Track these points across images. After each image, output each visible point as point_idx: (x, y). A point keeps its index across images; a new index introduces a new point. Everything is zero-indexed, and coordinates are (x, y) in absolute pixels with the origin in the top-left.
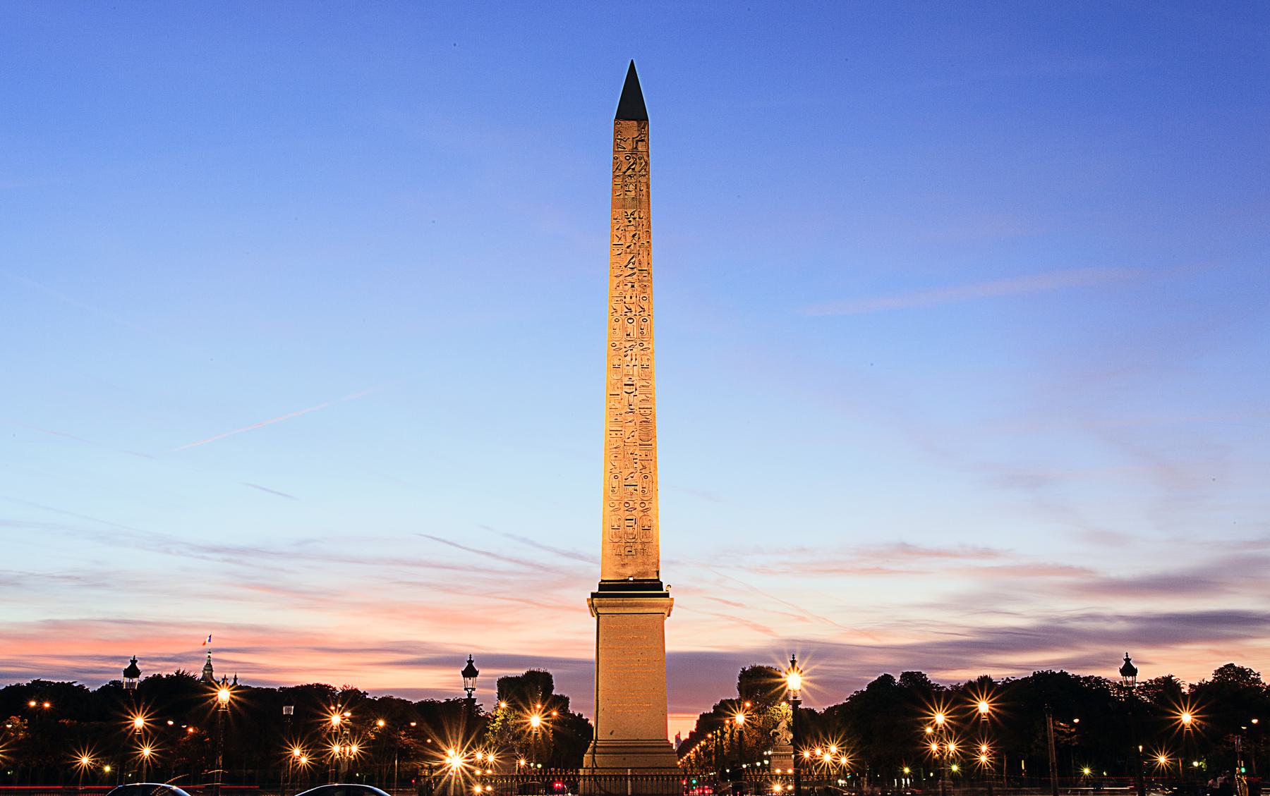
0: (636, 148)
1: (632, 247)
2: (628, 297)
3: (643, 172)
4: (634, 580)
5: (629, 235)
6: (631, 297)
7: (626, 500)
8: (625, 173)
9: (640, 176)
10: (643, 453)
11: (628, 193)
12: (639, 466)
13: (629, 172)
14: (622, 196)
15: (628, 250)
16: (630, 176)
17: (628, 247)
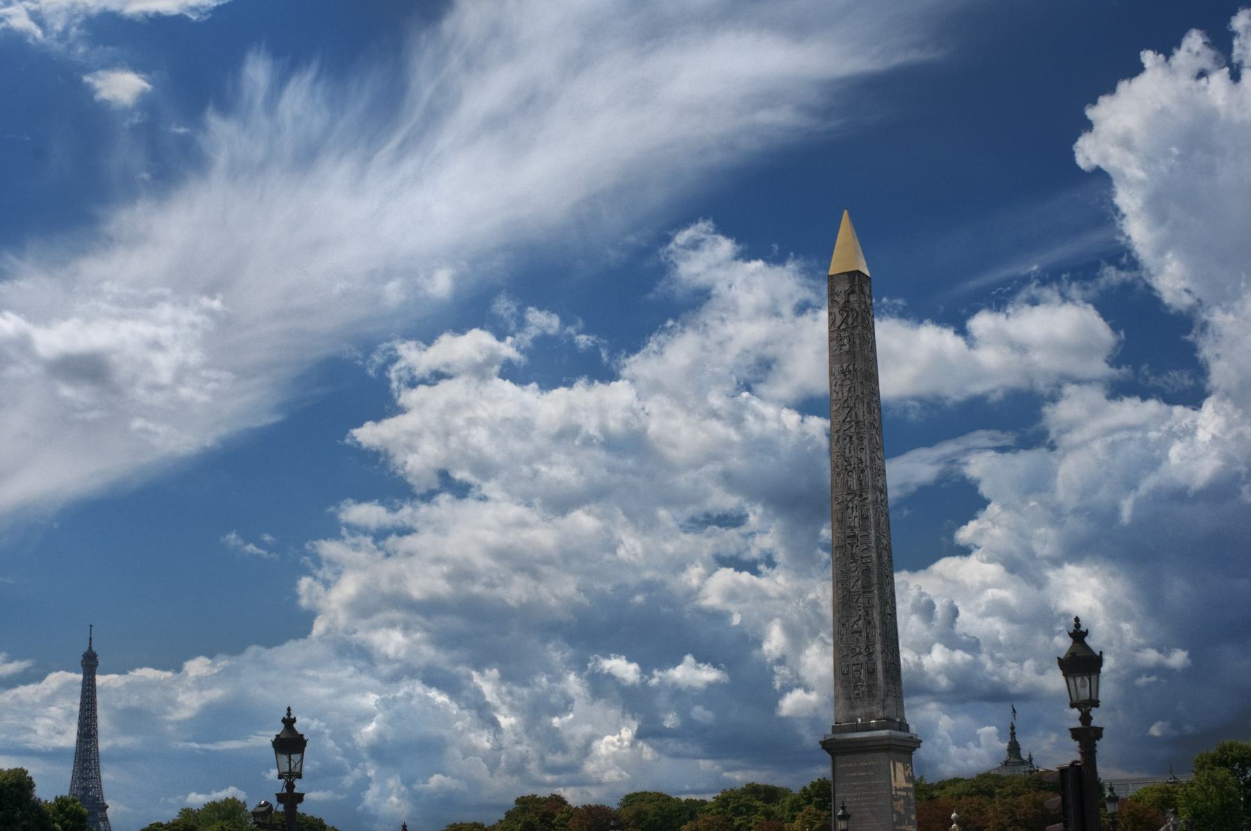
0: (848, 301)
2: (847, 451)
3: (855, 324)
5: (845, 389)
6: (850, 452)
7: (853, 646)
9: (853, 328)
11: (843, 348)
13: (842, 327)
14: (838, 352)
15: (845, 405)
16: (844, 330)
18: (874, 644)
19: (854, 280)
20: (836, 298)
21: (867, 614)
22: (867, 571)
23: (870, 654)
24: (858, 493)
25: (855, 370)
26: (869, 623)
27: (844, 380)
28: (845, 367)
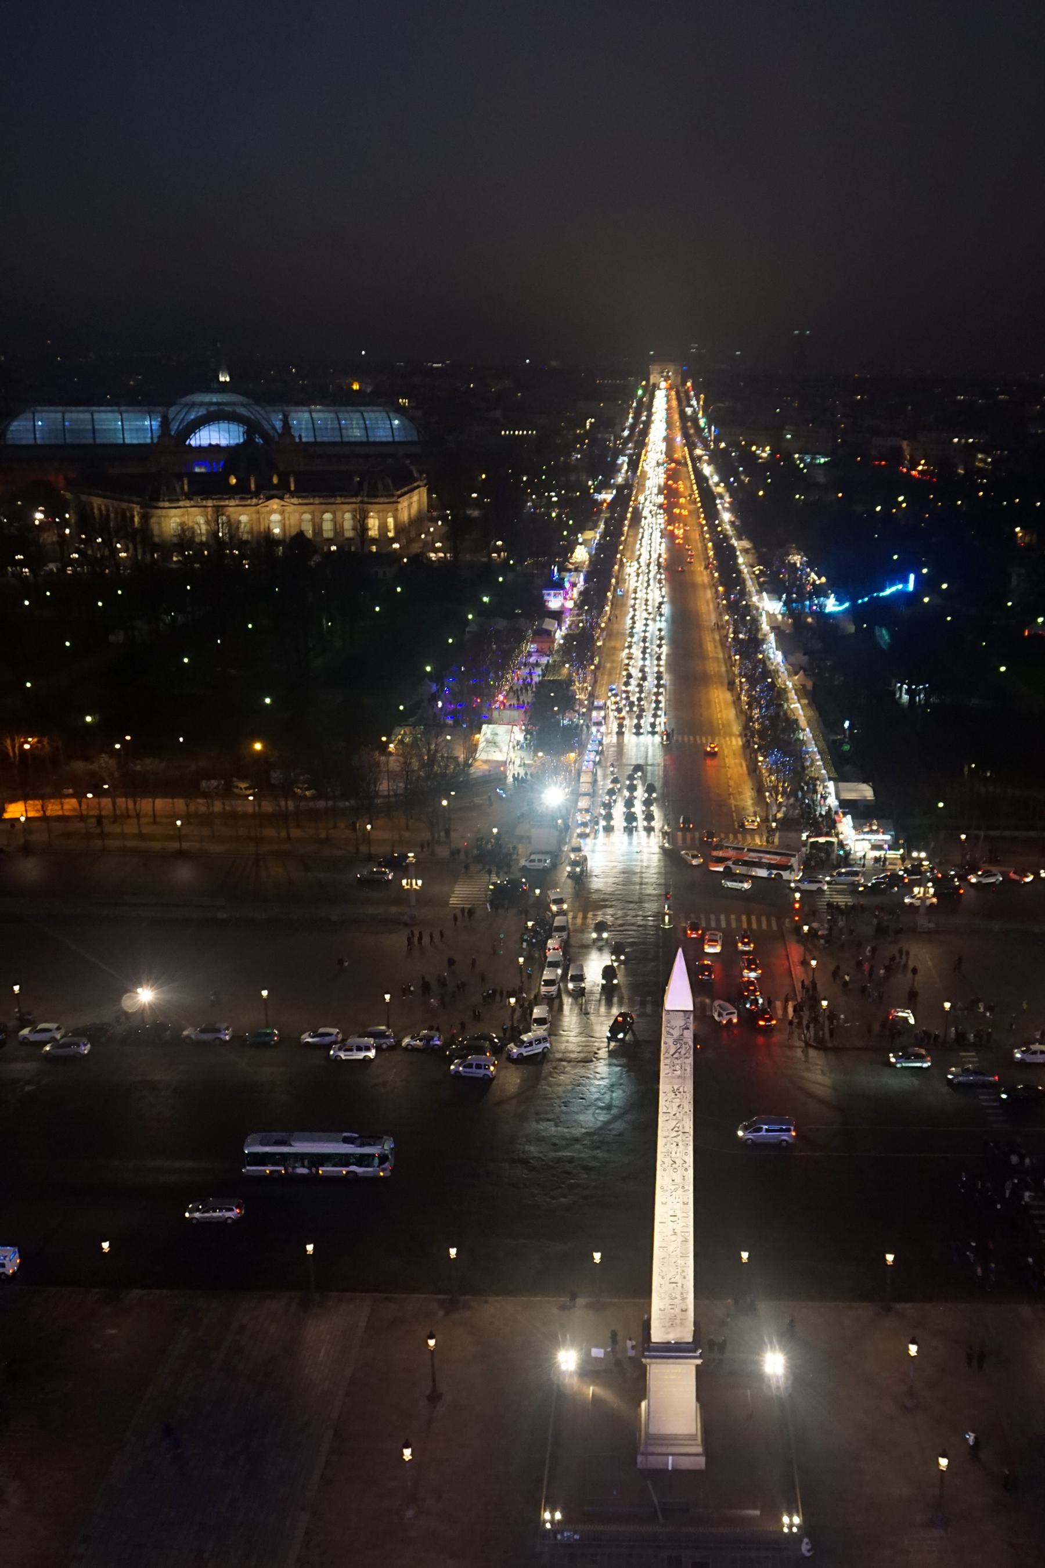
0: (682, 1035)
1: (678, 1115)
2: (673, 1153)
3: (687, 1055)
4: (676, 1343)
5: (675, 1105)
8: (672, 1055)
9: (687, 1058)
10: (683, 1262)
11: (675, 1072)
12: (680, 1270)
13: (676, 1055)
14: (670, 1075)
15: (674, 1117)
16: (677, 1058)
17: (674, 1115)
18: (687, 1293)
19: (689, 1018)
20: (671, 1031)
21: (683, 1271)
22: (686, 1241)
23: (683, 1299)
24: (681, 1185)
25: (684, 1092)
26: (685, 1278)
27: (674, 1098)
28: (675, 1089)
